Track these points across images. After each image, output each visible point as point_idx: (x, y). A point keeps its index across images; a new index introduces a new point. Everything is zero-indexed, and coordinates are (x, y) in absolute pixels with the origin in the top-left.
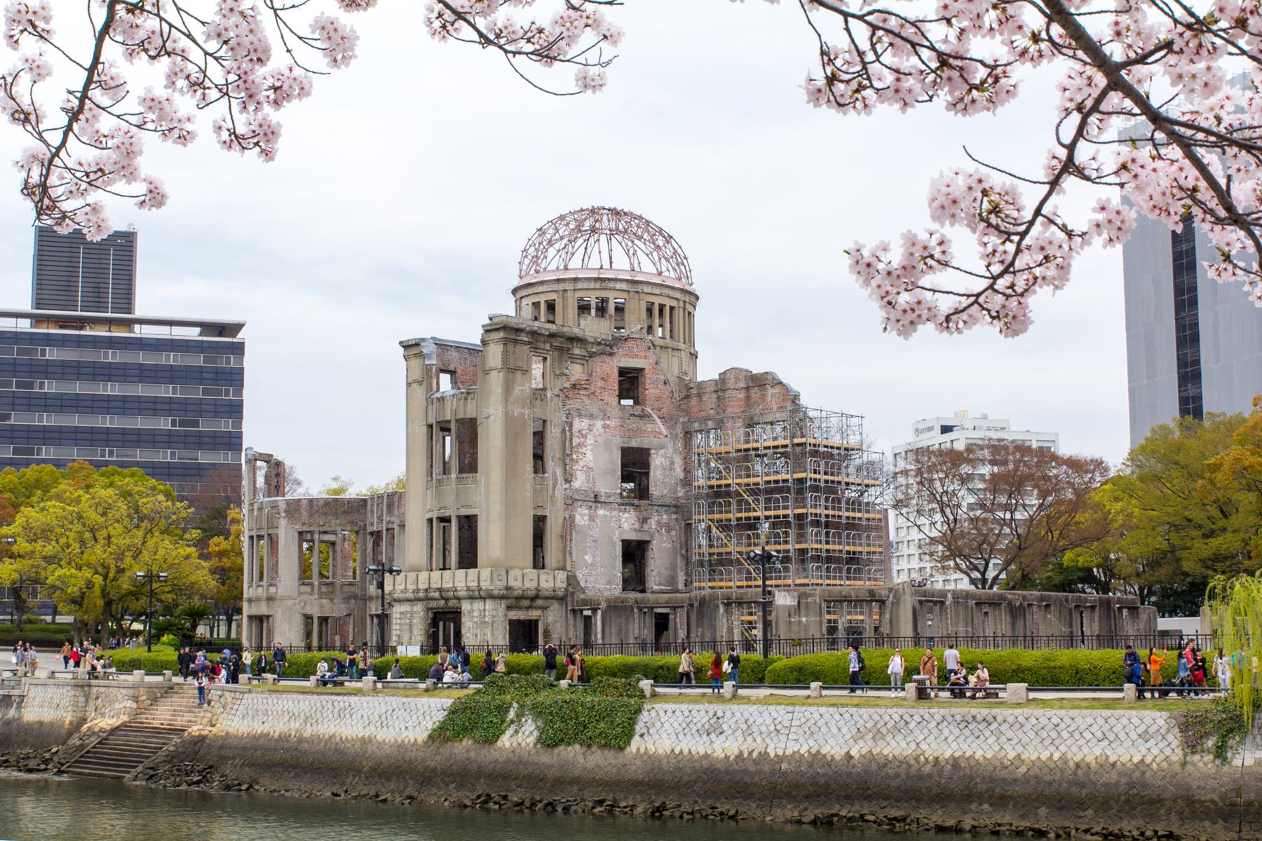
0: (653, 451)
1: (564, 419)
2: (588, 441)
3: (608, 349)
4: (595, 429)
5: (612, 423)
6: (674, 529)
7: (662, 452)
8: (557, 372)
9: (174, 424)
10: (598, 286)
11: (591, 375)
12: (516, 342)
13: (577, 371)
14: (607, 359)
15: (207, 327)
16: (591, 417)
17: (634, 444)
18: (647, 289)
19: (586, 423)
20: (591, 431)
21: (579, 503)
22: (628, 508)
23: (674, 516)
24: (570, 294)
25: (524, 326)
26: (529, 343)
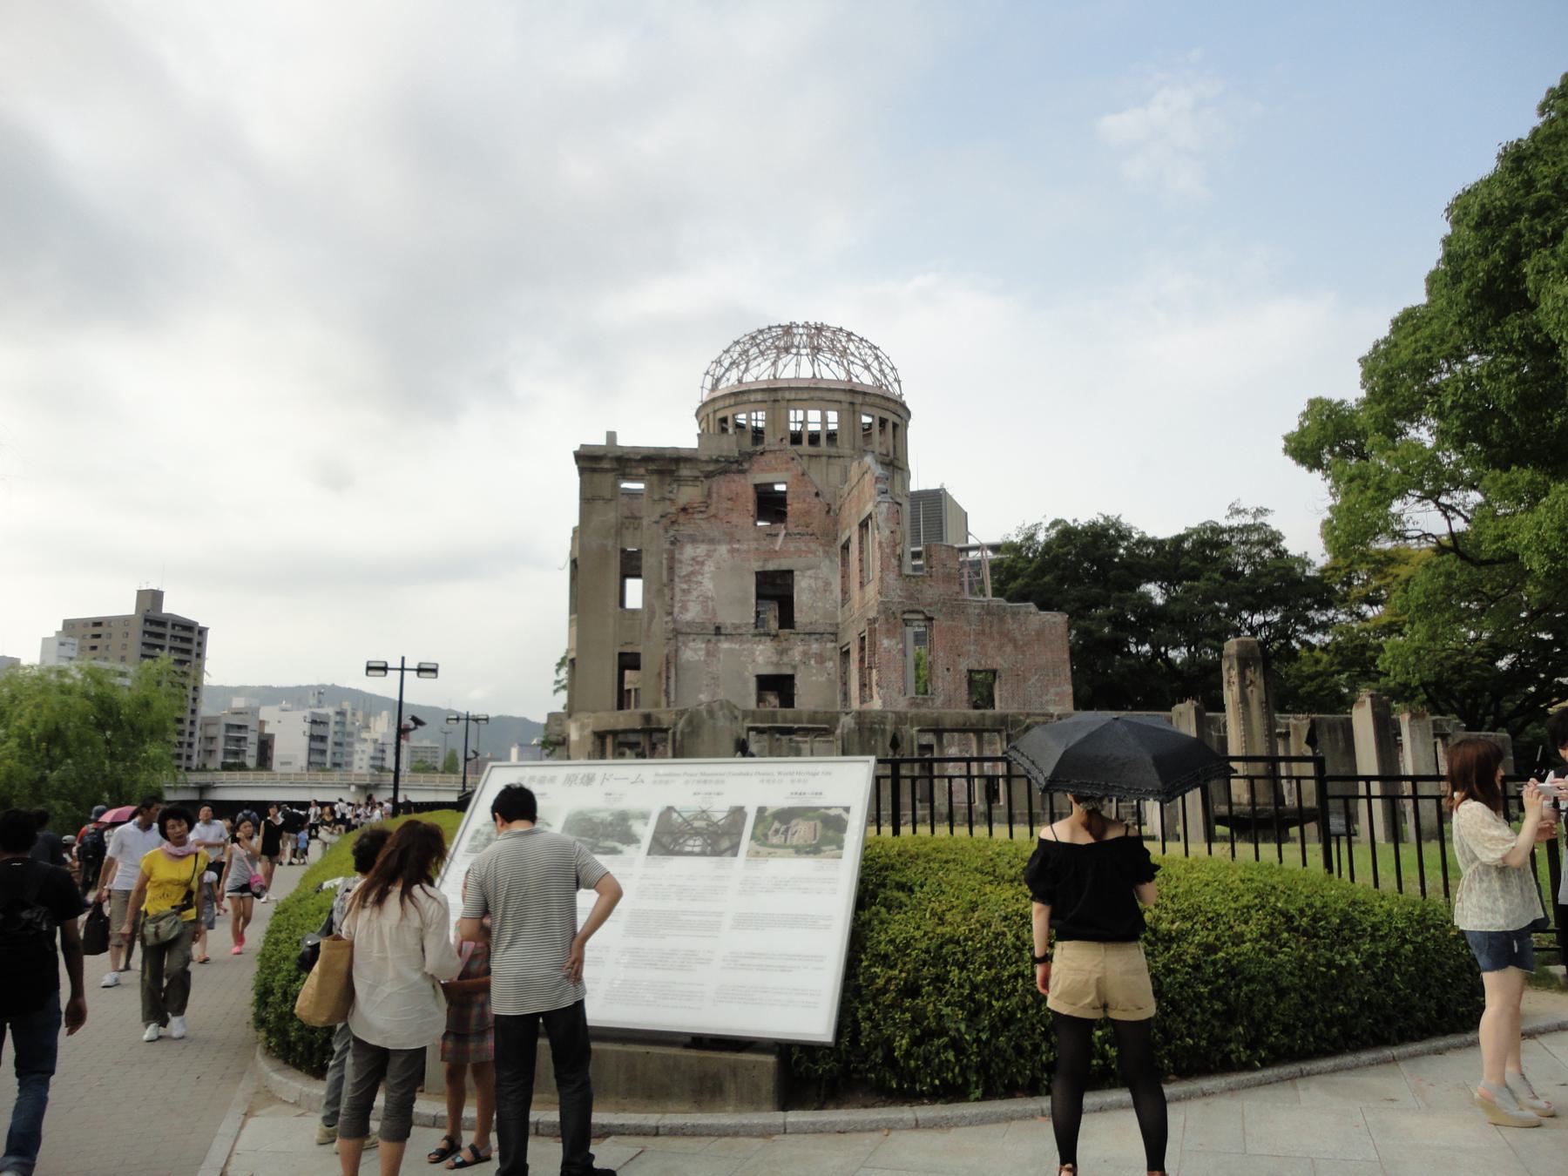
0: (795, 573)
1: (667, 546)
2: (706, 568)
3: (735, 466)
4: (717, 555)
5: (744, 547)
6: (830, 660)
7: (809, 573)
8: (656, 497)
10: (732, 401)
11: (709, 495)
12: (594, 470)
13: (688, 494)
14: (737, 477)
16: (712, 541)
17: (771, 566)
18: (787, 395)
19: (702, 549)
20: (710, 557)
21: (691, 637)
22: (763, 639)
23: (830, 645)
24: (711, 416)
25: (601, 453)
26: (613, 470)
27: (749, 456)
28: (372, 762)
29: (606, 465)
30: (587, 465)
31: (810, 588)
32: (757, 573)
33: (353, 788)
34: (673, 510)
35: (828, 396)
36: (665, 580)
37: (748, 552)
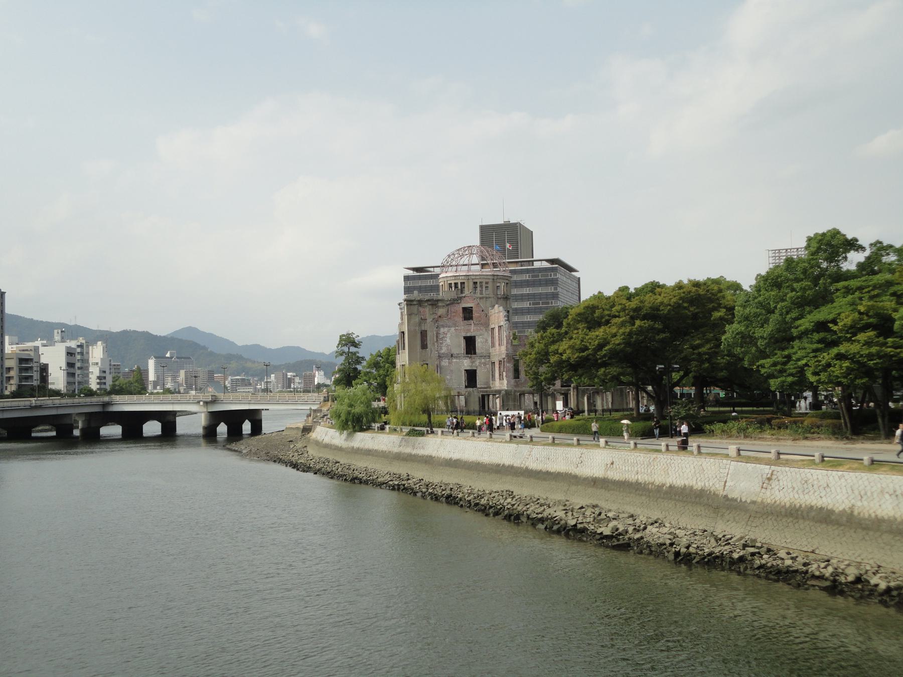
9: (530, 304)
11: (448, 312)
12: (411, 305)
13: (441, 311)
15: (547, 261)
16: (449, 327)
17: (468, 335)
19: (446, 329)
23: (488, 360)
27: (461, 298)
28: (98, 381)
29: (415, 303)
30: (409, 303)
31: (481, 342)
32: (465, 338)
33: (201, 403)
34: (436, 317)
35: (486, 277)
36: (435, 340)
37: (461, 330)
